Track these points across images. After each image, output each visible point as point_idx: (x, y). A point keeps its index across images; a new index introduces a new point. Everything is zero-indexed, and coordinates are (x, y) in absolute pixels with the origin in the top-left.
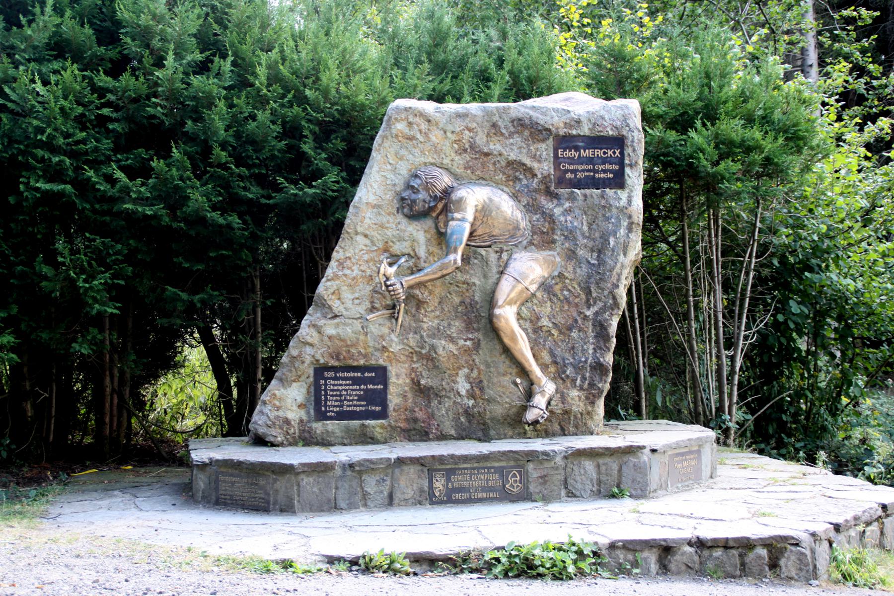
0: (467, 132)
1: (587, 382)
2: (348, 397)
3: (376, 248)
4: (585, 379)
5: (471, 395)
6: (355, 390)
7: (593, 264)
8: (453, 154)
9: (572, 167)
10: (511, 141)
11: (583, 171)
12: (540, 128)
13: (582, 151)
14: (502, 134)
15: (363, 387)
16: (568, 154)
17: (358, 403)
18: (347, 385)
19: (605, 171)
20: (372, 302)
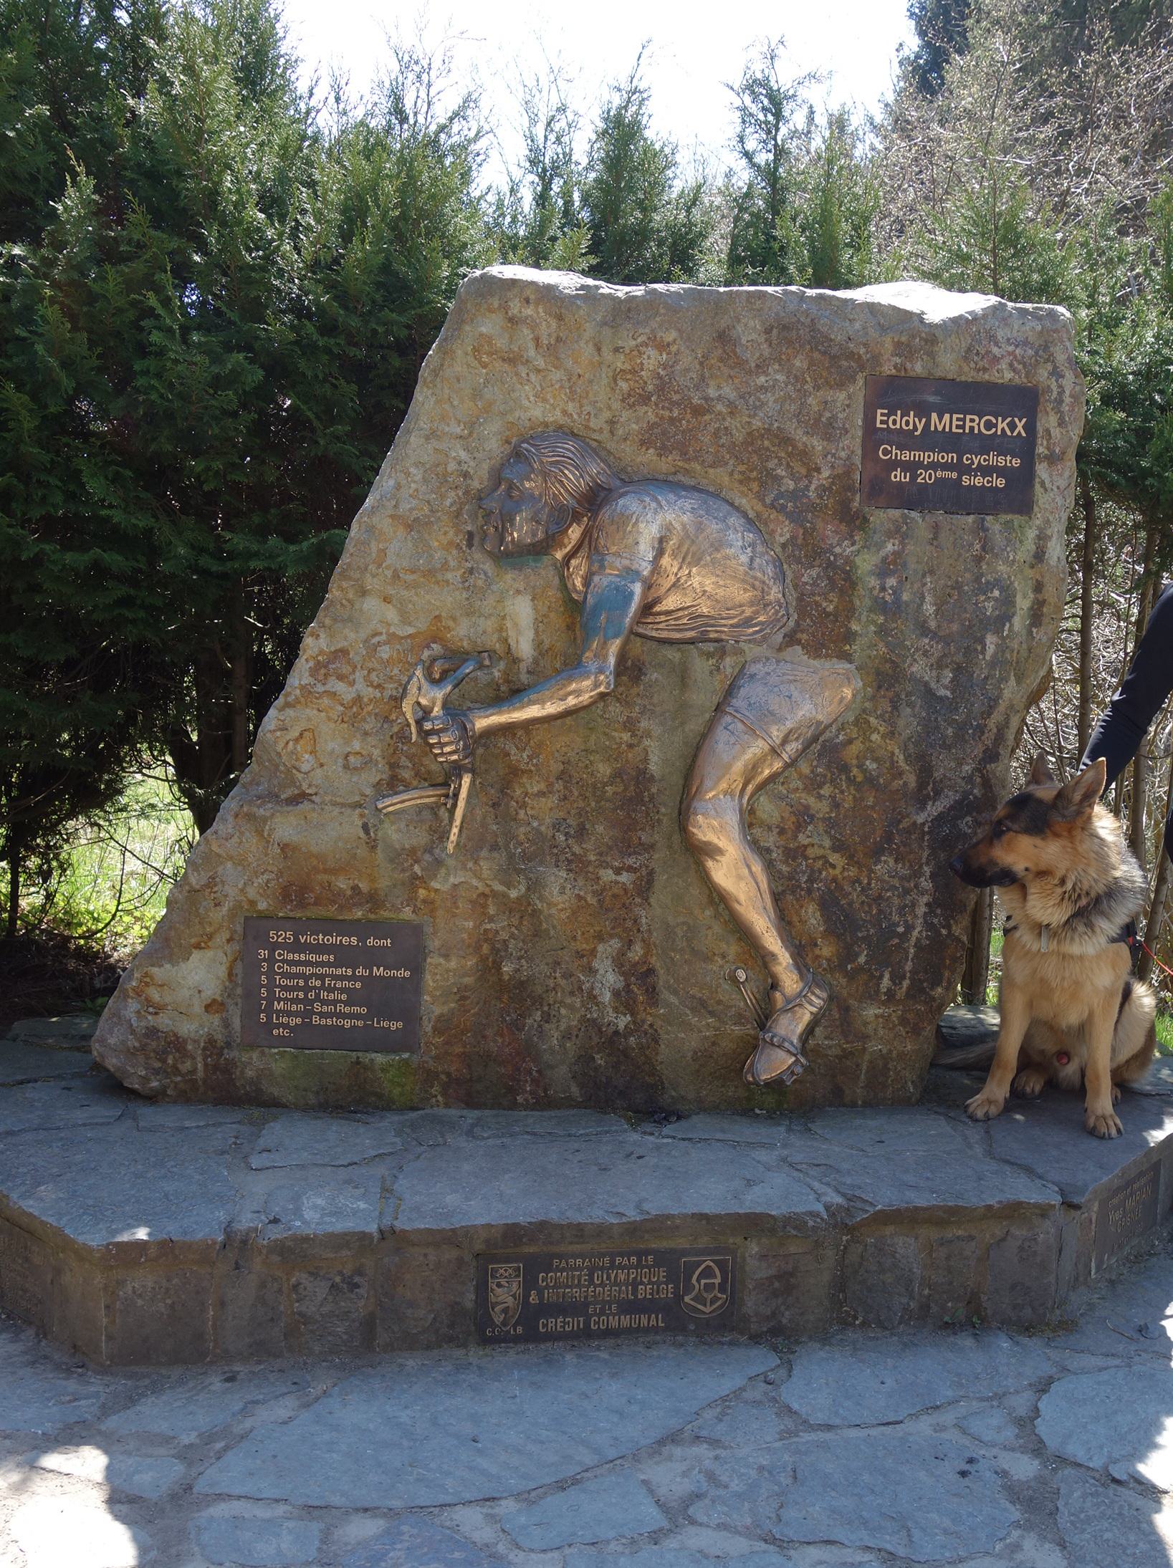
0: (651, 352)
1: (906, 983)
2: (324, 995)
3: (411, 631)
4: (904, 977)
5: (624, 1000)
6: (342, 978)
7: (941, 699)
8: (616, 405)
9: (906, 456)
10: (762, 380)
11: (934, 466)
12: (835, 350)
13: (934, 416)
14: (740, 363)
15: (360, 971)
16: (900, 421)
17: (347, 1010)
18: (322, 964)
19: (986, 471)
20: (393, 766)
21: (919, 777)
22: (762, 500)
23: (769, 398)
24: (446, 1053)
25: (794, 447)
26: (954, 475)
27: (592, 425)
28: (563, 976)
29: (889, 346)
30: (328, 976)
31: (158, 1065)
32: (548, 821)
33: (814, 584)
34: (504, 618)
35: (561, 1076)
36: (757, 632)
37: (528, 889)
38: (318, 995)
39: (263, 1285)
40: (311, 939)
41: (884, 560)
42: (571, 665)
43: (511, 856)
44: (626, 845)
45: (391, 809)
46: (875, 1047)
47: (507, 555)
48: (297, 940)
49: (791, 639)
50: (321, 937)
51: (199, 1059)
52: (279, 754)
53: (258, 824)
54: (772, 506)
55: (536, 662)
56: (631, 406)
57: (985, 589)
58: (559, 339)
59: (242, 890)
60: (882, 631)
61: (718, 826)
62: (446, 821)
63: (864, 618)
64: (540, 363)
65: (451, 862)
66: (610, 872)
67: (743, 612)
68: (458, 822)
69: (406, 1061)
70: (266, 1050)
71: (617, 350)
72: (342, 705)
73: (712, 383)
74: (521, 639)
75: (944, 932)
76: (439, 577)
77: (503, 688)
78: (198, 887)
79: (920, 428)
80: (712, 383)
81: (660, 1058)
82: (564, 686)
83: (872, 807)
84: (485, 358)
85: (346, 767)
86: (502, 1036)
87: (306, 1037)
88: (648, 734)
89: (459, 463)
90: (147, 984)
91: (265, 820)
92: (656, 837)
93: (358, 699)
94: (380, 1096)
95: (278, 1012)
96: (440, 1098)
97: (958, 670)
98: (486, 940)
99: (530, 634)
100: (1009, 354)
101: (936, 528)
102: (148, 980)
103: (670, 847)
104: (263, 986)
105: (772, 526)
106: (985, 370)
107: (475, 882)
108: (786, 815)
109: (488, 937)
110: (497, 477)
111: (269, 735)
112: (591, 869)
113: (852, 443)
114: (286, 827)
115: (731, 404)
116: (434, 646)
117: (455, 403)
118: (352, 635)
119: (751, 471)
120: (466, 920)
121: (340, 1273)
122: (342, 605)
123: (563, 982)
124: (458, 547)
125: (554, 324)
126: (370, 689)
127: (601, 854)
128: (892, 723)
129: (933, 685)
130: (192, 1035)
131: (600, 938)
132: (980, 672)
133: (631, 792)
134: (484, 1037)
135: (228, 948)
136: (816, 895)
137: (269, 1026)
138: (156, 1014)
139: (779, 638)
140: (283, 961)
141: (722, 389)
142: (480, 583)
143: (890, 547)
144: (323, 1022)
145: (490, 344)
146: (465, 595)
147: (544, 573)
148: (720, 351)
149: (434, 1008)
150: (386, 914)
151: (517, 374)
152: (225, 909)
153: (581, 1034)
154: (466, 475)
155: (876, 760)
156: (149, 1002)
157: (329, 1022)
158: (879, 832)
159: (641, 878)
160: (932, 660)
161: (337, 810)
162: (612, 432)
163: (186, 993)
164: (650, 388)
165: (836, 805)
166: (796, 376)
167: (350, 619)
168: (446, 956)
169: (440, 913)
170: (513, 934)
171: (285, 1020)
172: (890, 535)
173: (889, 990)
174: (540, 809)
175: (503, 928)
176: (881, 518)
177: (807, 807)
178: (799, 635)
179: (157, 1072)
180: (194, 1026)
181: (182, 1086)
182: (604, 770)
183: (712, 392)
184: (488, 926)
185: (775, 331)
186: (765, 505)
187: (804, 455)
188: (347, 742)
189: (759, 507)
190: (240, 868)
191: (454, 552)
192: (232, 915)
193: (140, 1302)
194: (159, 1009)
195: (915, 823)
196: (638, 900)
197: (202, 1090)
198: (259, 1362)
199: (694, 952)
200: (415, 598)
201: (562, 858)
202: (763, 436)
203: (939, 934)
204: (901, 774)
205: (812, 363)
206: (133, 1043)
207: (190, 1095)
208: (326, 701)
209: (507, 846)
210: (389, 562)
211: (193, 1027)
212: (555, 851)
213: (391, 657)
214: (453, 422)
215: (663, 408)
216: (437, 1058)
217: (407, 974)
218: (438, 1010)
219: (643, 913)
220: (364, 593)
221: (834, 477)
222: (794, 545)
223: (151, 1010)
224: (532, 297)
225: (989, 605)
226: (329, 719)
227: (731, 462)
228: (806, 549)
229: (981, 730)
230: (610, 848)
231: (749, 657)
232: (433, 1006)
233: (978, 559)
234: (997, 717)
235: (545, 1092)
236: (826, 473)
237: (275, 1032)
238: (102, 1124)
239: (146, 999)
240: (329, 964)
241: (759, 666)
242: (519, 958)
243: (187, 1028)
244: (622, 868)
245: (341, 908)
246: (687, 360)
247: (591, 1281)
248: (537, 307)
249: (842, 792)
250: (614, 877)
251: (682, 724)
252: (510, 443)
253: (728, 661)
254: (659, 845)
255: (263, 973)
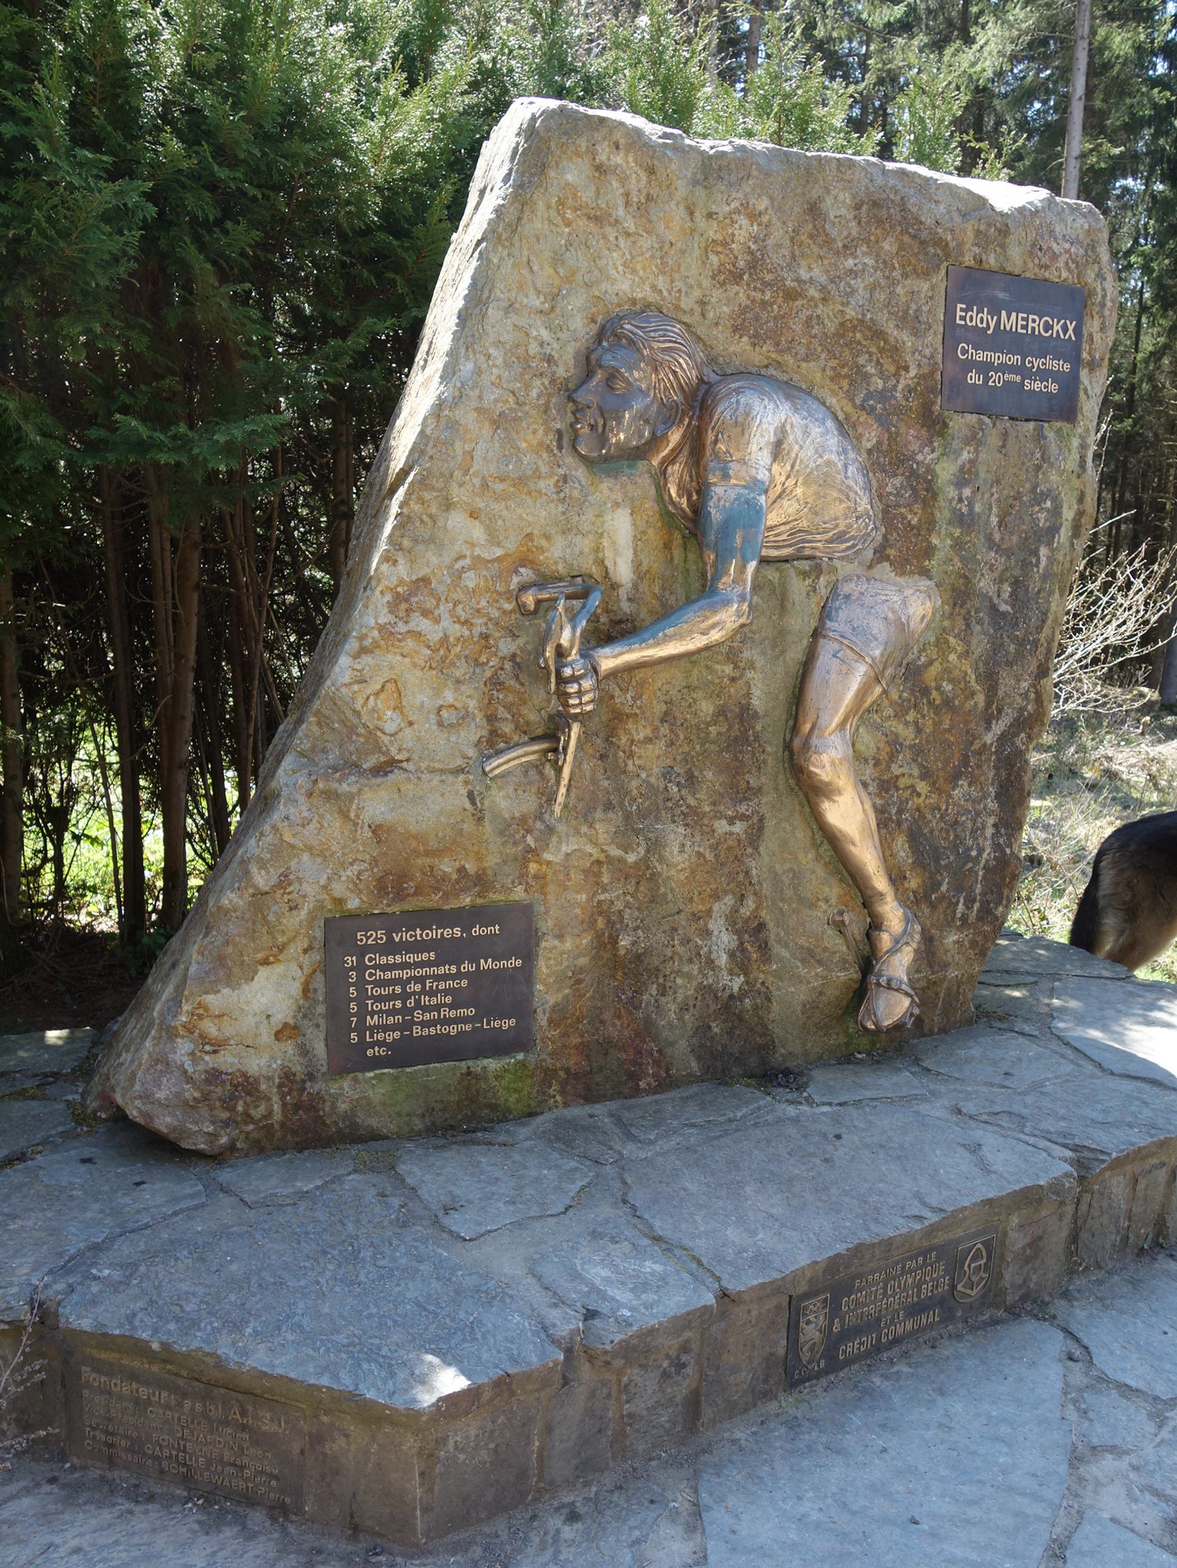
0: (743, 221)
1: (977, 906)
2: (424, 1000)
3: (499, 552)
4: (974, 901)
5: (740, 962)
6: (445, 977)
7: (1004, 615)
8: (706, 283)
9: (980, 356)
10: (850, 262)
11: (1003, 368)
12: (924, 235)
13: (1004, 313)
14: (828, 242)
15: (466, 967)
16: (980, 318)
17: (453, 1014)
18: (422, 964)
19: (1044, 375)
20: (491, 719)
21: (987, 696)
22: (852, 400)
23: (859, 284)
24: (565, 1046)
25: (886, 341)
26: (1018, 379)
27: (683, 305)
28: (682, 944)
29: (970, 234)
30: (429, 977)
31: (225, 1115)
32: (656, 770)
33: (898, 494)
34: (601, 535)
35: (682, 1053)
36: (849, 548)
37: (648, 851)
38: (418, 1002)
39: (592, 1395)
40: (407, 936)
41: (962, 469)
42: (703, 589)
43: (628, 816)
44: (740, 792)
45: (497, 772)
46: (953, 973)
47: (607, 459)
48: (390, 939)
49: (881, 554)
50: (418, 932)
51: (275, 1099)
52: (357, 714)
53: (340, 803)
54: (863, 408)
55: (635, 586)
56: (722, 284)
57: (1038, 499)
58: (649, 198)
59: (325, 887)
60: (958, 545)
61: (830, 761)
62: (553, 781)
63: (943, 532)
64: (630, 224)
65: (561, 828)
66: (724, 822)
67: (837, 526)
68: (565, 782)
69: (523, 1065)
70: (359, 1075)
71: (710, 215)
72: (429, 647)
73: (803, 263)
74: (619, 560)
75: (1008, 851)
76: (532, 486)
77: (603, 619)
78: (267, 889)
79: (992, 326)
80: (803, 263)
81: (771, 1017)
82: (707, 618)
83: (949, 730)
84: (569, 215)
85: (440, 724)
86: (619, 1017)
87: (406, 1054)
88: (752, 665)
89: (542, 345)
90: (201, 1017)
91: (351, 797)
92: (763, 779)
93: (445, 639)
94: (493, 1107)
95: (372, 1029)
96: (558, 1098)
97: (1016, 584)
98: (600, 913)
99: (628, 554)
100: (1068, 251)
101: (1005, 435)
102: (201, 1011)
103: (776, 789)
104: (352, 1000)
105: (860, 430)
106: (1047, 267)
107: (589, 849)
108: (882, 745)
109: (601, 909)
110: (588, 365)
111: (344, 690)
112: (706, 821)
113: (934, 339)
114: (376, 803)
115: (823, 289)
116: (522, 570)
117: (535, 268)
118: (434, 560)
119: (843, 367)
120: (578, 892)
121: (667, 1356)
122: (422, 521)
123: (680, 950)
124: (549, 449)
125: (644, 177)
126: (457, 626)
127: (714, 804)
128: (968, 644)
129: (996, 601)
130: (264, 1072)
131: (716, 897)
132: (1034, 585)
133: (735, 732)
134: (602, 1022)
135: (306, 960)
136: (905, 826)
137: (363, 1045)
138: (215, 1052)
139: (869, 554)
140: (375, 967)
141: (813, 272)
142: (576, 493)
143: (965, 456)
144: (426, 1032)
145: (575, 197)
146: (561, 508)
147: (641, 481)
148: (810, 226)
149: (548, 997)
150: (494, 897)
151: (605, 237)
152: (303, 913)
153: (699, 1003)
154: (550, 359)
155: (951, 681)
156: (204, 1039)
157: (433, 1031)
158: (957, 756)
159: (751, 827)
160: (996, 575)
161: (438, 778)
162: (703, 315)
163: (251, 1021)
164: (741, 264)
165: (919, 731)
166: (885, 262)
167: (432, 540)
168: (560, 937)
169: (551, 888)
170: (628, 903)
171: (381, 1036)
172: (967, 441)
173: (963, 914)
174: (649, 759)
175: (618, 897)
176: (960, 423)
177: (897, 735)
178: (889, 551)
179: (226, 1124)
180: (263, 1061)
181: (255, 1135)
182: (707, 708)
183: (804, 275)
184: (602, 897)
185: (865, 207)
186: (855, 406)
187: (895, 351)
188: (437, 693)
189: (849, 408)
190: (319, 860)
191: (545, 455)
192: (312, 918)
193: (462, 1457)
194: (217, 1046)
195: (985, 745)
196: (749, 850)
197: (279, 1135)
198: (587, 1484)
199: (801, 900)
200: (505, 513)
201: (678, 811)
202: (855, 327)
203: (1003, 852)
204: (973, 694)
205: (901, 248)
206: (191, 1093)
207: (266, 1144)
208: (410, 643)
209: (621, 804)
210: (475, 467)
211: (263, 1062)
212: (670, 804)
213: (477, 586)
214: (532, 292)
215: (755, 288)
216: (553, 1054)
217: (519, 963)
218: (552, 999)
219: (753, 864)
220: (448, 505)
221: (921, 377)
222: (879, 451)
223: (207, 1048)
224: (622, 141)
225: (1042, 516)
226: (415, 665)
227: (823, 356)
228: (887, 460)
229: (1035, 643)
230: (722, 795)
231: (841, 574)
232: (547, 994)
233: (1038, 468)
234: (1046, 631)
235: (667, 1070)
236: (913, 372)
237: (370, 1052)
238: (196, 1208)
239: (201, 1036)
240: (429, 964)
241: (852, 585)
242: (635, 929)
243: (256, 1064)
244: (735, 818)
245: (446, 895)
246: (778, 234)
247: (885, 1294)
248: (627, 155)
249: (923, 717)
250: (728, 828)
251: (783, 652)
252: (593, 321)
253: (823, 580)
254: (765, 788)
255: (352, 985)
